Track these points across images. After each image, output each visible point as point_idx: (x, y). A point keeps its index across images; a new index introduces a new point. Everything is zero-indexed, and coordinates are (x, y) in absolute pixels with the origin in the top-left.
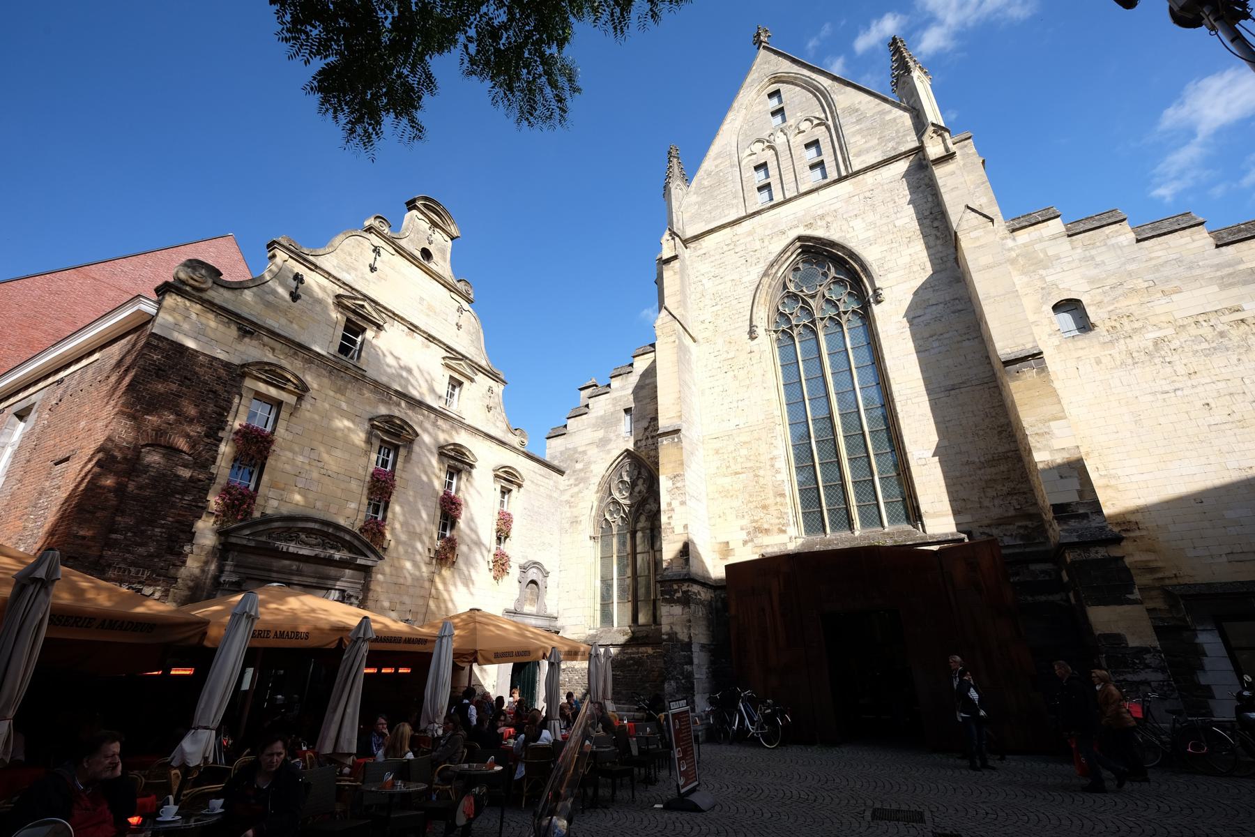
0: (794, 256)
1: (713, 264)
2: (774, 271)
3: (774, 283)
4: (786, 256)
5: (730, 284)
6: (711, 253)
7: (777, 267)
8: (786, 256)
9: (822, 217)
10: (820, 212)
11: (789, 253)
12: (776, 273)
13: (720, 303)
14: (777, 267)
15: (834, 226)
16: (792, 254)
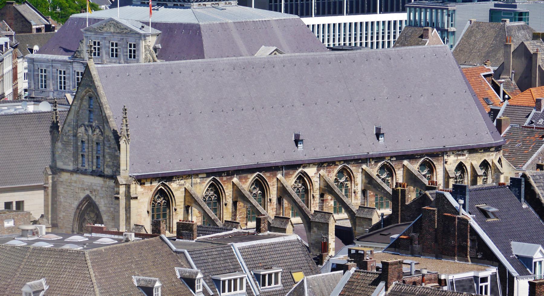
0: (87, 203)
1: (64, 190)
2: (80, 207)
3: (81, 212)
4: (84, 203)
5: (68, 204)
6: (64, 183)
7: (81, 206)
8: (84, 203)
9: (95, 191)
10: (95, 187)
11: (85, 202)
12: (82, 207)
13: (66, 212)
14: (81, 206)
15: (97, 197)
16: (86, 202)
